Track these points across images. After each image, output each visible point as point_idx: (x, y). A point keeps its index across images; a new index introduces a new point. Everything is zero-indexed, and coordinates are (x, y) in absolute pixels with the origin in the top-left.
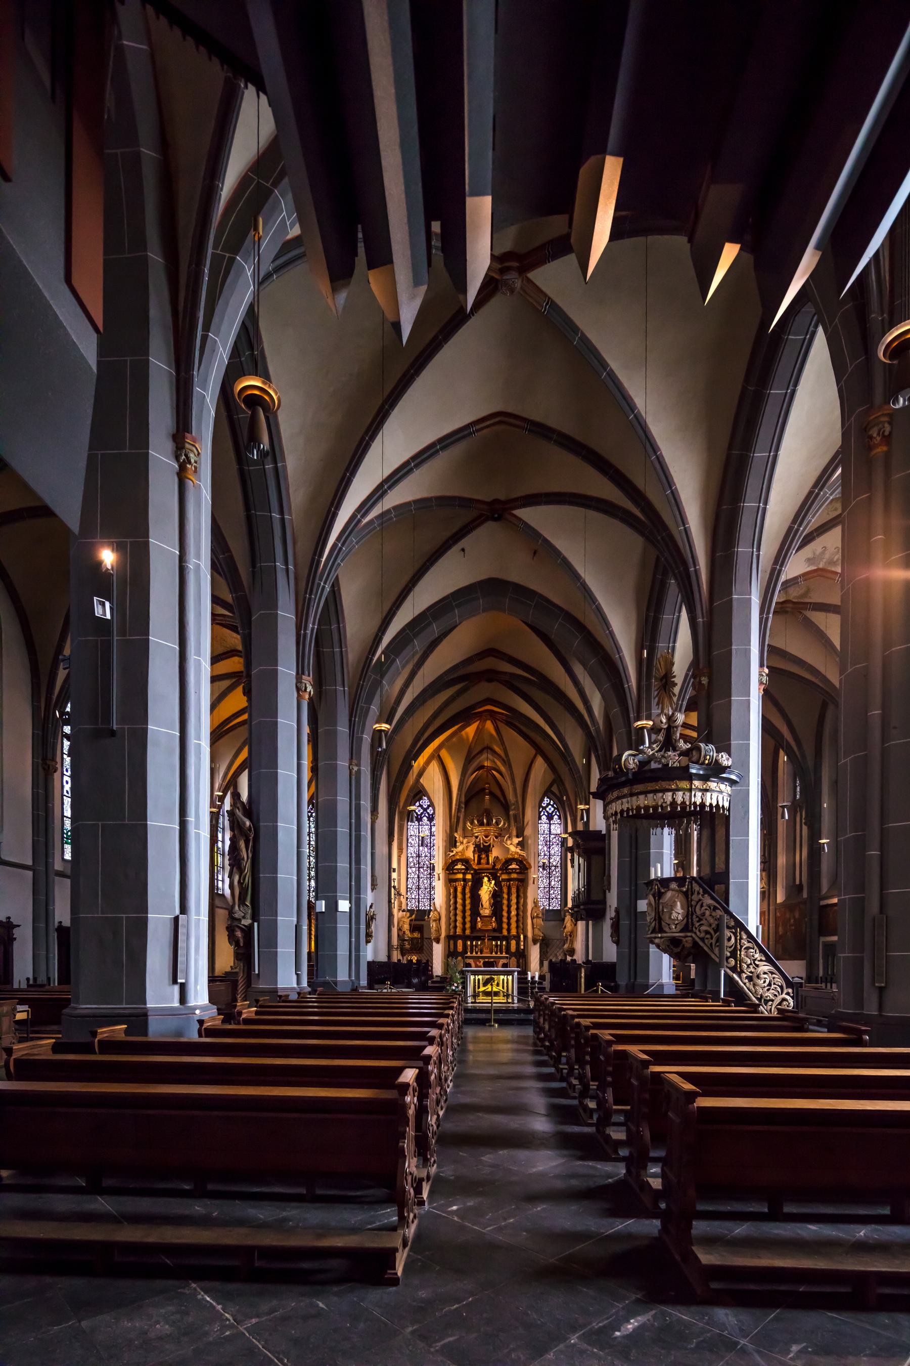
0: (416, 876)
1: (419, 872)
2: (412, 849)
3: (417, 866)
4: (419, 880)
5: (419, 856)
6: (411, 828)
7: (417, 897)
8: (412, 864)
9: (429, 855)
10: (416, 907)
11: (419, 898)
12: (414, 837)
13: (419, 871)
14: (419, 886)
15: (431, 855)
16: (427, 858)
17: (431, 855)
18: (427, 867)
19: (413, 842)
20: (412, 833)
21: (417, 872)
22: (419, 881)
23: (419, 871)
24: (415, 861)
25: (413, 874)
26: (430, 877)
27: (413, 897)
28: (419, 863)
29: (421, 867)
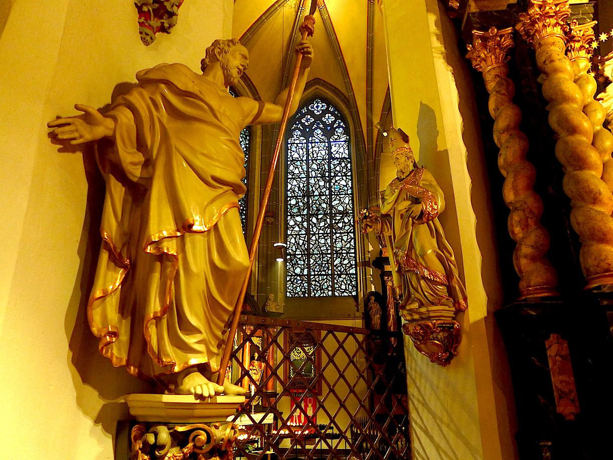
0: (303, 232)
1: (309, 225)
2: (295, 183)
3: (305, 212)
4: (309, 239)
5: (308, 194)
6: (294, 149)
7: (306, 272)
8: (295, 210)
9: (327, 192)
10: (304, 293)
11: (309, 275)
12: (298, 163)
13: (308, 221)
14: (308, 249)
15: (331, 191)
16: (323, 198)
17: (331, 191)
18: (325, 214)
19: (296, 171)
20: (296, 156)
21: (305, 224)
22: (308, 242)
23: (308, 221)
24: (301, 204)
25: (297, 229)
26: (331, 232)
27: (298, 271)
28: (308, 208)
29: (313, 215)
